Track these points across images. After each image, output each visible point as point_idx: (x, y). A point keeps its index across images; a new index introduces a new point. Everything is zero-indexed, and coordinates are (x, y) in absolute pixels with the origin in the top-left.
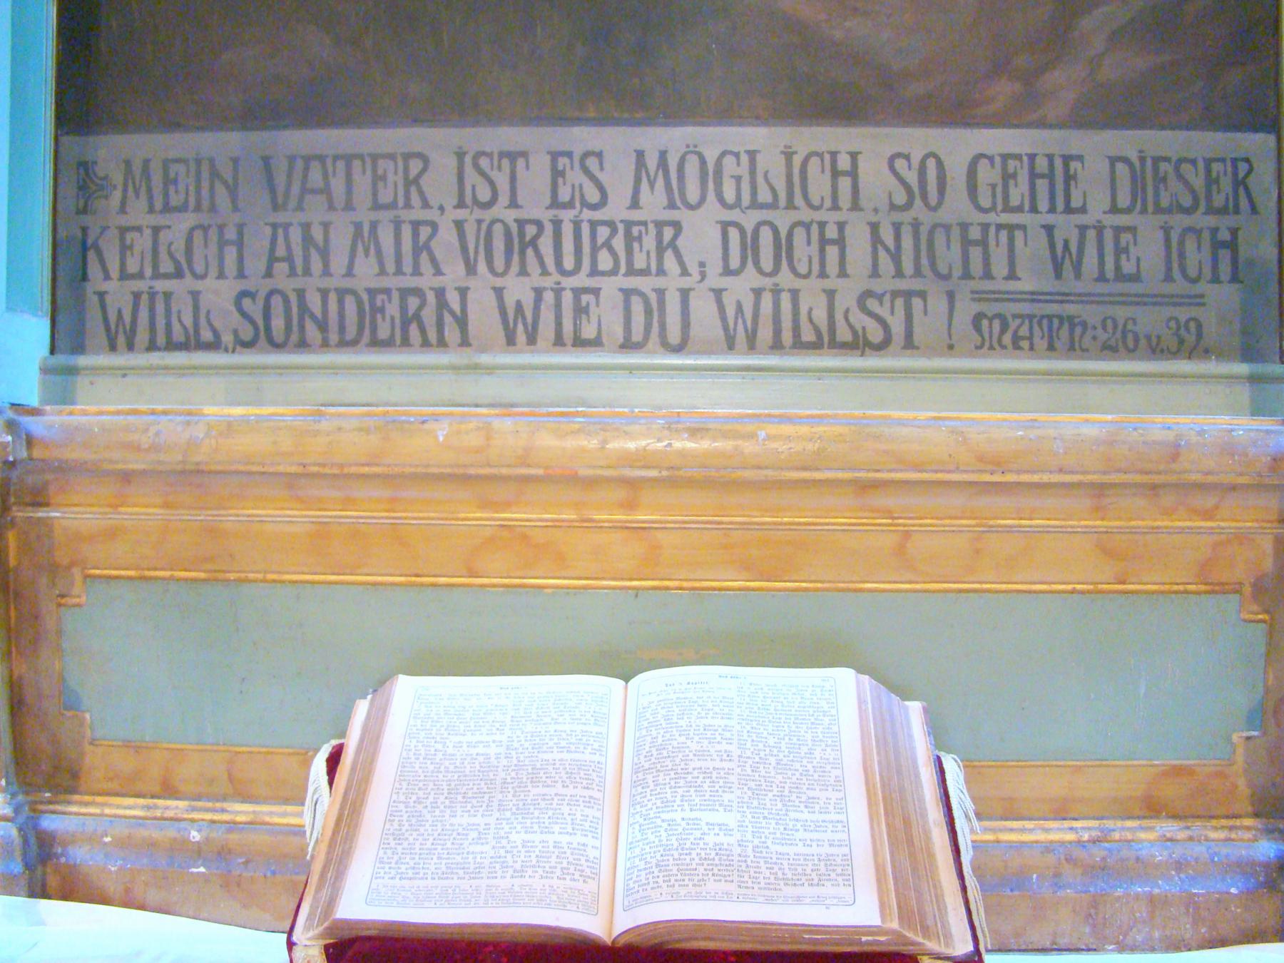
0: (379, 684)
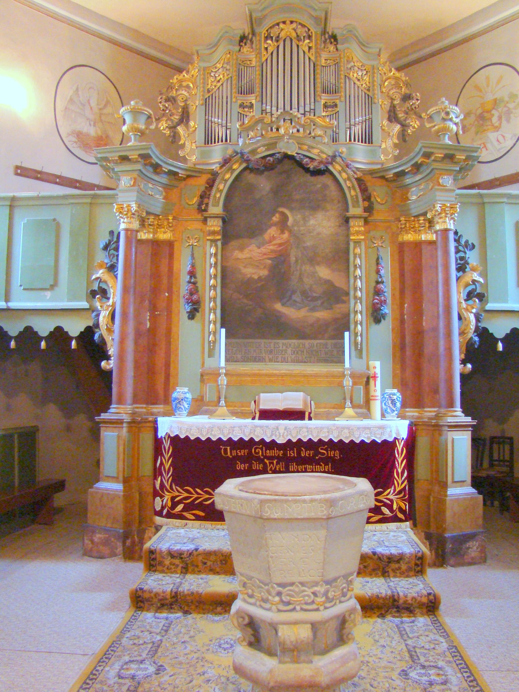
0: (259, 395)
